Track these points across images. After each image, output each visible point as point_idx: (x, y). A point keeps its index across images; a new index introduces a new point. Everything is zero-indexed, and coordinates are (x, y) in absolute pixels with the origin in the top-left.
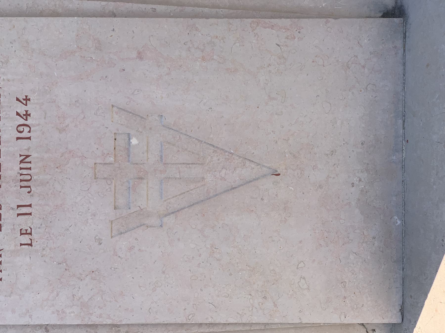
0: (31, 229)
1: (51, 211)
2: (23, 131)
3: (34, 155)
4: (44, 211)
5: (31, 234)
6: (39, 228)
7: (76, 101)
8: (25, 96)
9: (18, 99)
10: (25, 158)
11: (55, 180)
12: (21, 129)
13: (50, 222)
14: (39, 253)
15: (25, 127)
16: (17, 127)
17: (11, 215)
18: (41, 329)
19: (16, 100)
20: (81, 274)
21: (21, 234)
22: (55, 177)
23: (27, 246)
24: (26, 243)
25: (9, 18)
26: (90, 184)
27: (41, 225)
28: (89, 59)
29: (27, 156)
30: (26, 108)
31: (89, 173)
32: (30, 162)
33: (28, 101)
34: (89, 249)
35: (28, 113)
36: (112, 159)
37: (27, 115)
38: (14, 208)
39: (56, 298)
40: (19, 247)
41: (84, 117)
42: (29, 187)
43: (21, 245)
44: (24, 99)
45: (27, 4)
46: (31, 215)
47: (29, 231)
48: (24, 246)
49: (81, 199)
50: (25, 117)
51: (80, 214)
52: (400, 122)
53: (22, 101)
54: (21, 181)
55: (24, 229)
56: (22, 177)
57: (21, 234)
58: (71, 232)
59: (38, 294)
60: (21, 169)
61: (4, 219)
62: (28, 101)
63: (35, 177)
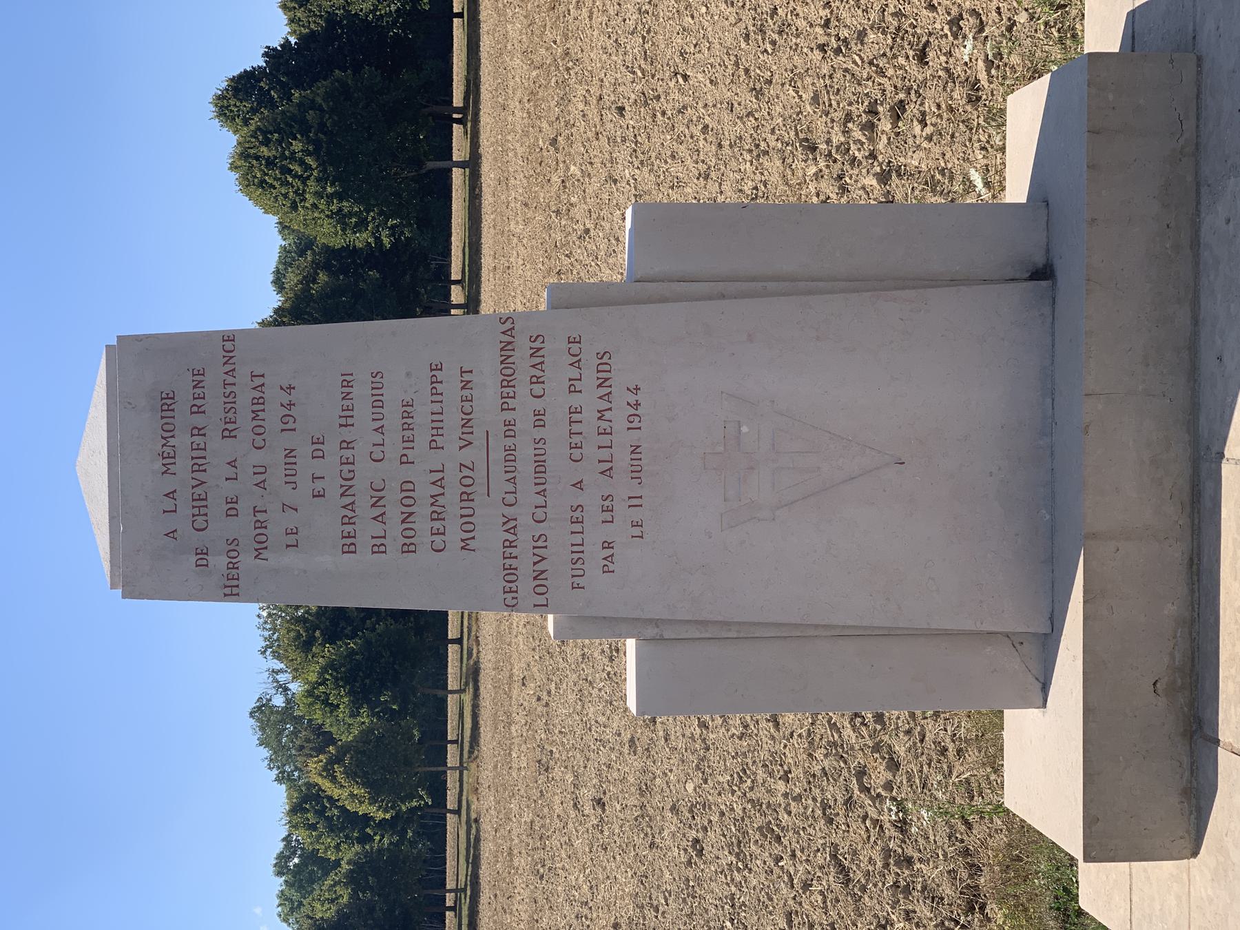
3: (644, 445)
9: (628, 389)
10: (635, 449)
12: (631, 419)
25: (619, 307)
29: (638, 447)
30: (636, 398)
36: (721, 449)
37: (638, 404)
43: (633, 537)
52: (1049, 401)
56: (633, 468)
63: (645, 468)
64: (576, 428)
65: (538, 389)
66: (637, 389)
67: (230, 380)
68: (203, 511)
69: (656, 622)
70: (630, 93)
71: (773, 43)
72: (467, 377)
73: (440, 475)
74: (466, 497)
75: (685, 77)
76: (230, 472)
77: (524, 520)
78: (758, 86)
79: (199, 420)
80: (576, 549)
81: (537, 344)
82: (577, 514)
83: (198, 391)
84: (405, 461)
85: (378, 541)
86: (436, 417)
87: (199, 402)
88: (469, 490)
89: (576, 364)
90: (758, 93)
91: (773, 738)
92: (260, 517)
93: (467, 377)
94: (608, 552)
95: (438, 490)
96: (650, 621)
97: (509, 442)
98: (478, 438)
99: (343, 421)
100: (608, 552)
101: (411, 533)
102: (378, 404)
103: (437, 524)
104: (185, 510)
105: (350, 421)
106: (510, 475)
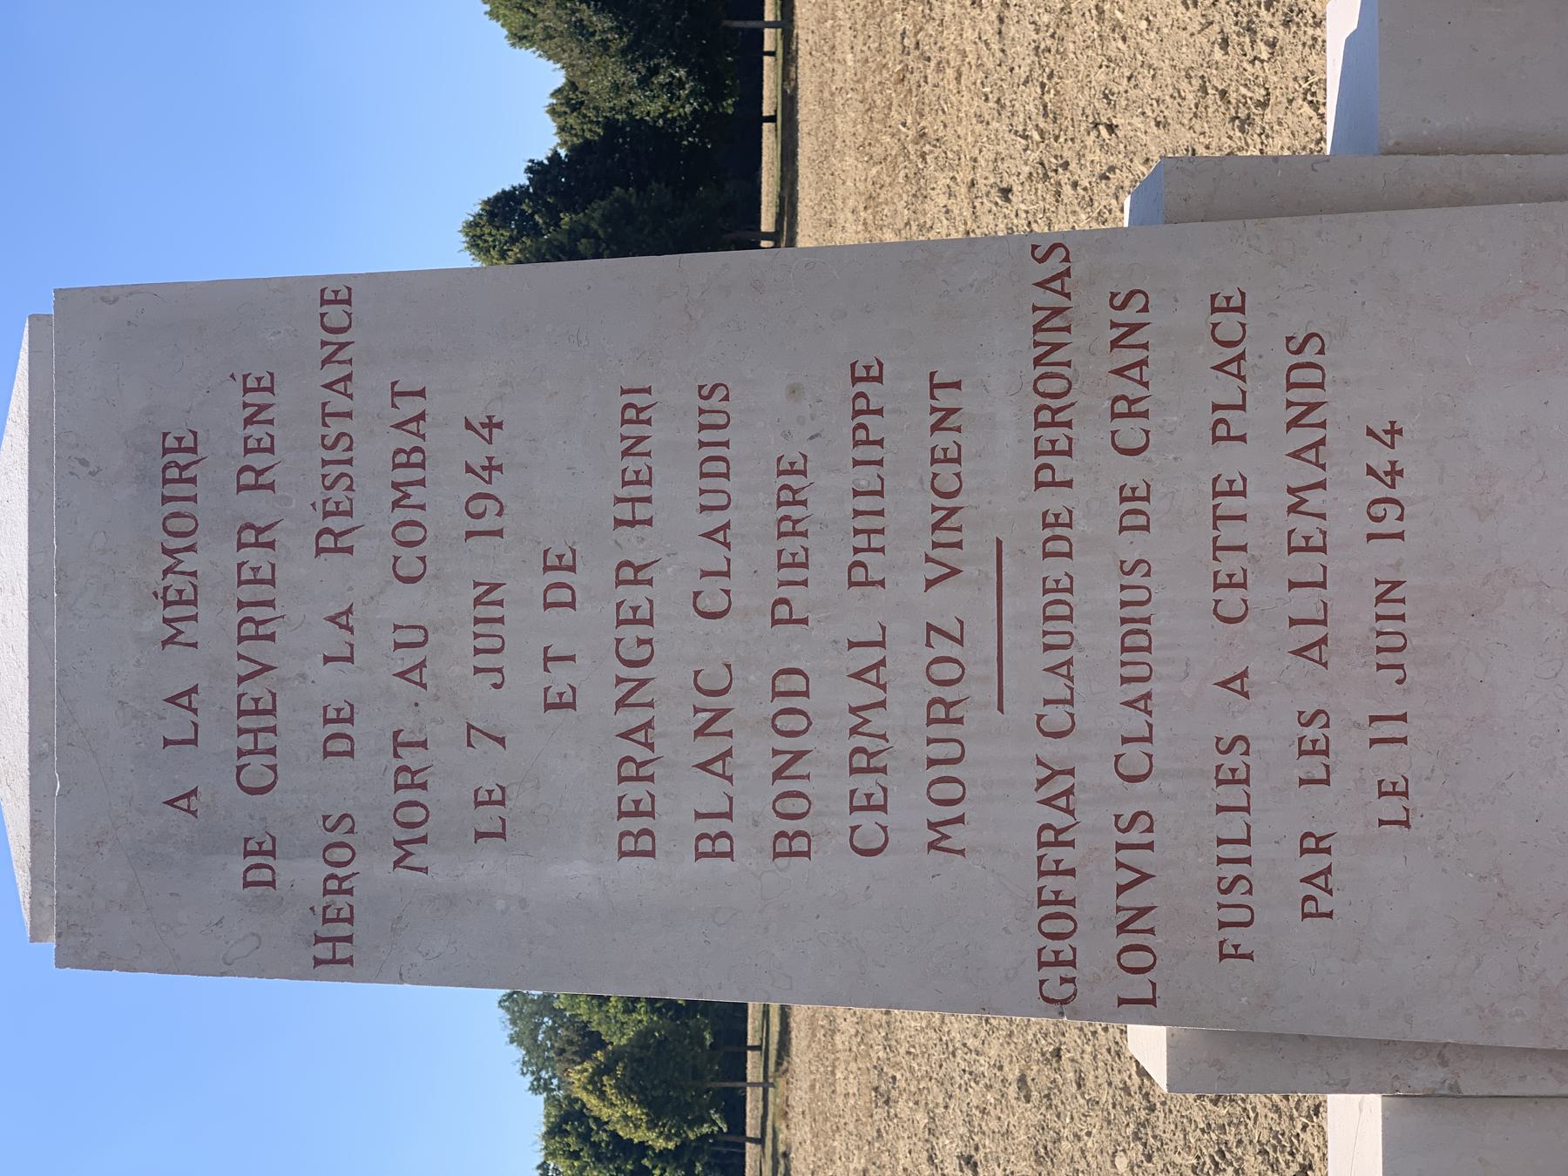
0: (1406, 780)
1: (1457, 734)
2: (1384, 517)
3: (1412, 580)
4: (1440, 733)
5: (1405, 794)
6: (1428, 779)
7: (1522, 432)
8: (1390, 422)
9: (1370, 432)
10: (1389, 590)
11: (1468, 649)
12: (1378, 510)
13: (1456, 764)
14: (1429, 848)
15: (1389, 505)
16: (1369, 507)
17: (1355, 742)
18: (1427, 1055)
19: (1367, 435)
20: (1540, 910)
21: (1382, 794)
22: (1467, 639)
23: (1396, 827)
24: (1393, 819)
25: (1347, 216)
26: (1561, 659)
27: (1433, 770)
28: (1557, 314)
29: (1396, 584)
30: (1392, 455)
31: (1559, 630)
32: (1403, 601)
33: (1396, 436)
34: (1560, 841)
35: (1398, 468)
37: (1395, 472)
38: (1361, 723)
39: (1474, 972)
40: (1376, 829)
41: (1544, 476)
42: (1401, 667)
43: (1382, 822)
44: (1386, 432)
45: (1385, 174)
46: (1406, 744)
47: (1400, 788)
48: (1388, 826)
49: (1538, 702)
50: (1388, 479)
51: (1534, 741)
53: (1382, 435)
54: (1380, 650)
55: (1388, 780)
56: (1383, 641)
57: (1382, 794)
58: (1511, 793)
59: (1428, 957)
60: (1379, 618)
61: (1336, 754)
62: (1396, 436)
63: (1414, 642)
64: (1230, 533)
65: (1131, 433)
66: (1394, 431)
67: (338, 403)
68: (265, 740)
69: (1440, 1052)
70: (1018, 168)
71: (1272, 44)
72: (946, 399)
73: (875, 654)
74: (943, 713)
75: (1111, 128)
76: (335, 640)
77: (1095, 775)
78: (1243, 113)
79: (257, 507)
80: (1229, 851)
81: (1130, 315)
82: (1234, 760)
83: (255, 431)
84: (784, 616)
85: (713, 827)
86: (864, 503)
87: (259, 461)
88: (949, 694)
89: (1233, 367)
90: (1245, 123)
91: (1277, 1110)
92: (411, 758)
93: (946, 399)
94: (1317, 862)
95: (868, 694)
96: (1425, 1048)
97: (1056, 569)
98: (975, 560)
99: (625, 512)
100: (1317, 862)
101: (798, 805)
102: (715, 466)
103: (867, 783)
104: (220, 738)
105: (642, 511)
106: (1059, 656)
